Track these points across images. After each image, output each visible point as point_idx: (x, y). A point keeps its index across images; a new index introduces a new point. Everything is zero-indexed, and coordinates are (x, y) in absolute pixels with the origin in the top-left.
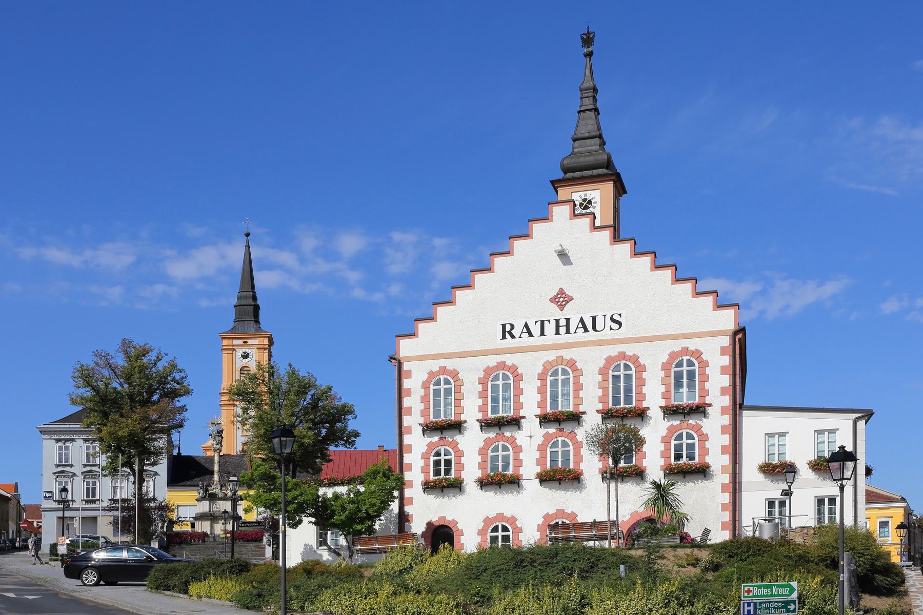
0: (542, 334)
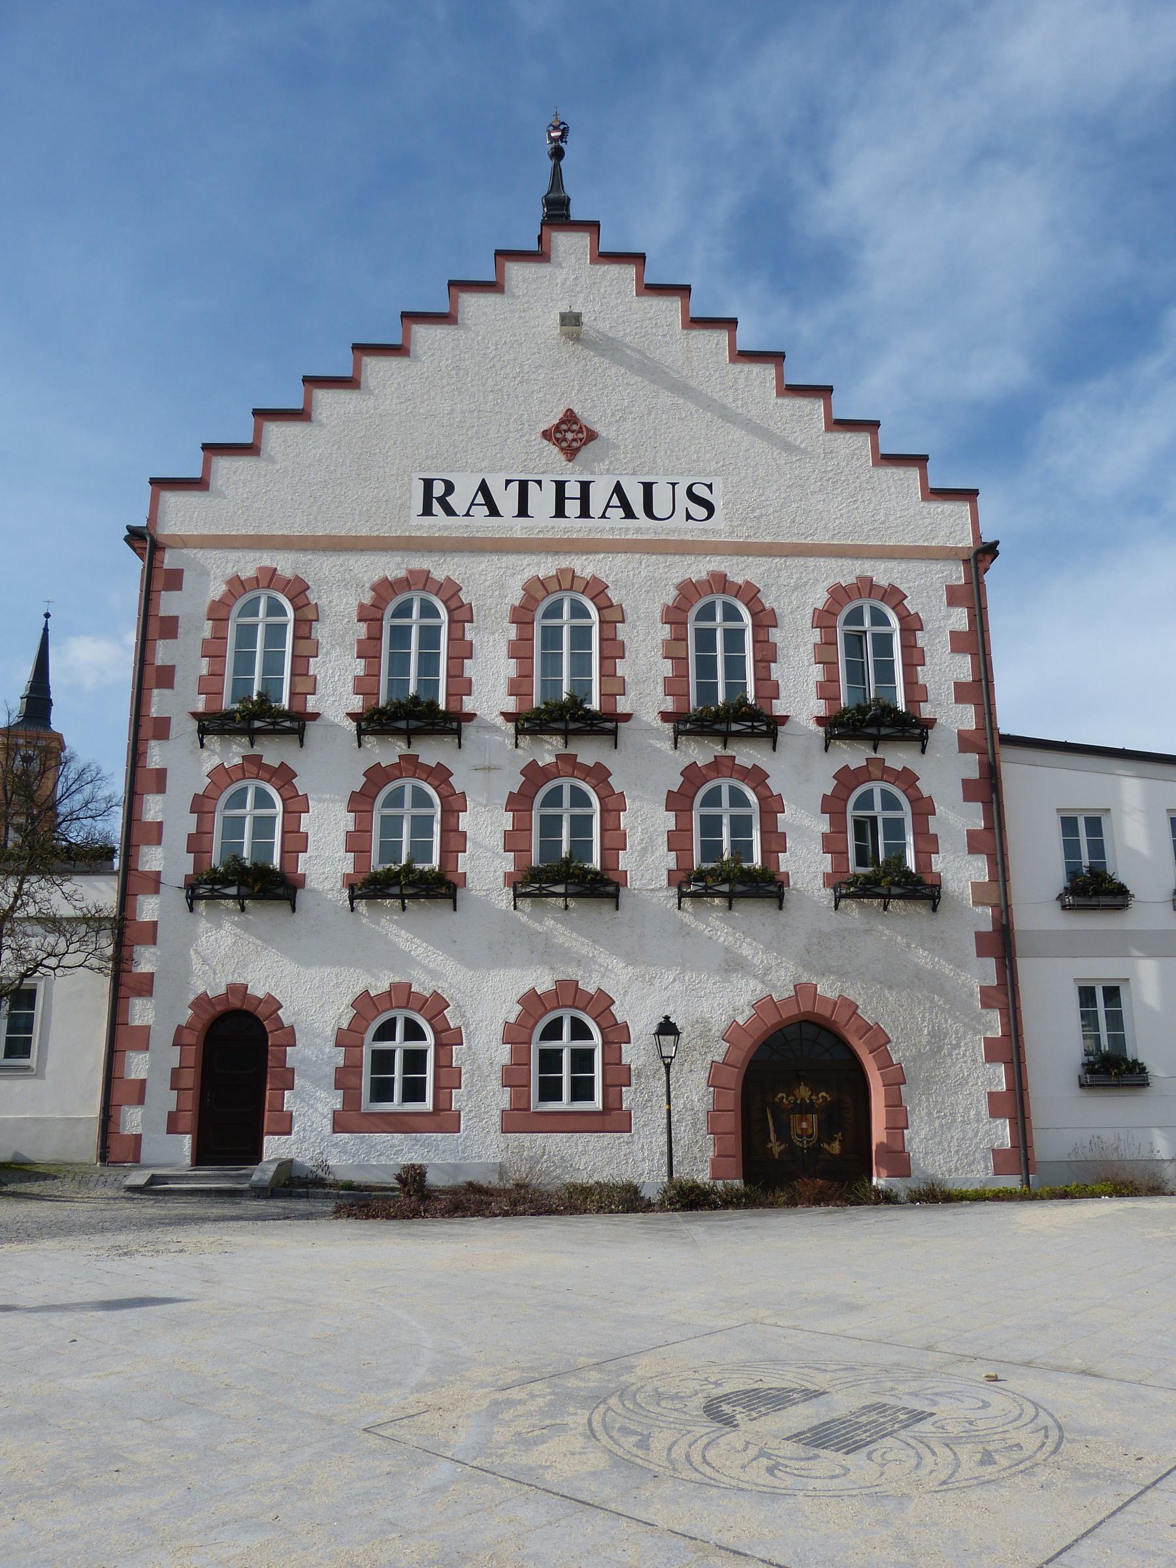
0: (523, 511)
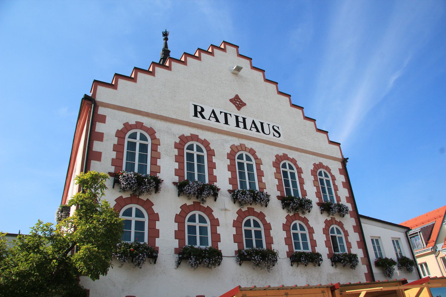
0: (226, 123)
